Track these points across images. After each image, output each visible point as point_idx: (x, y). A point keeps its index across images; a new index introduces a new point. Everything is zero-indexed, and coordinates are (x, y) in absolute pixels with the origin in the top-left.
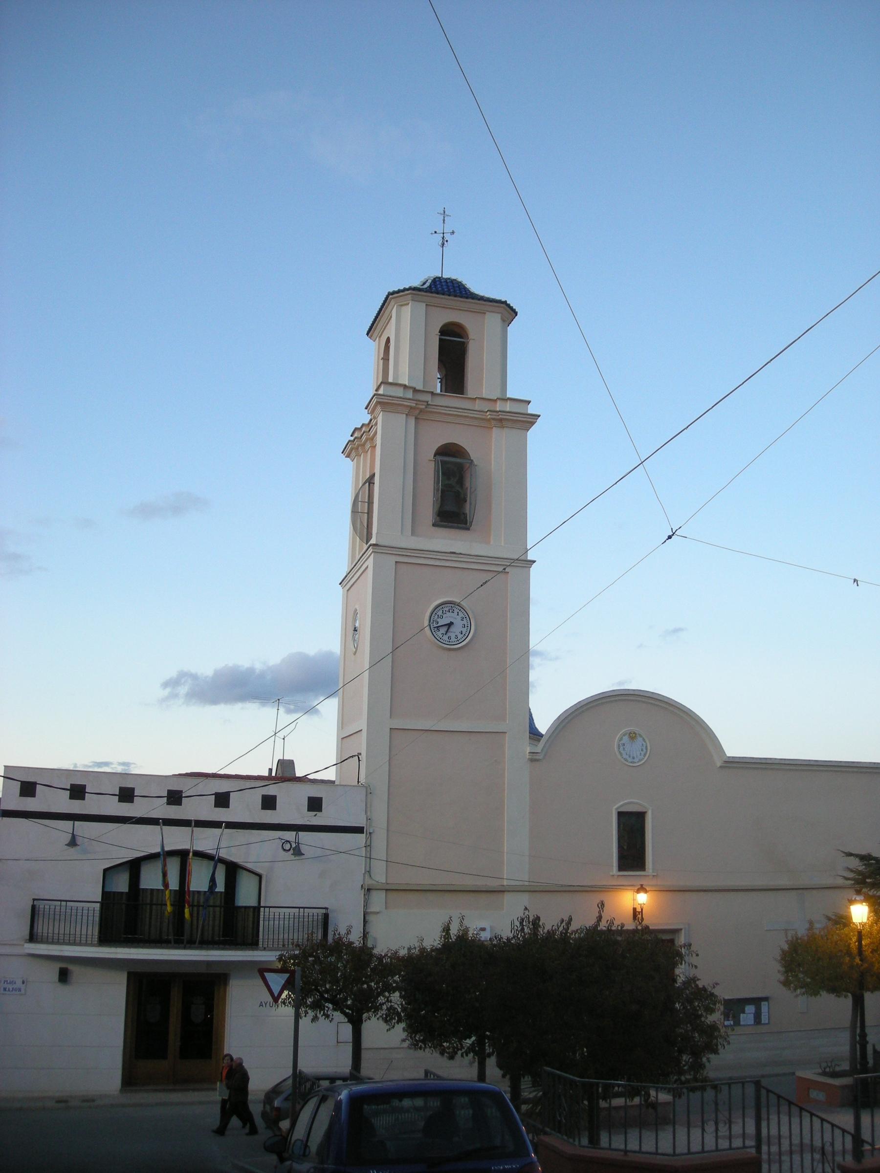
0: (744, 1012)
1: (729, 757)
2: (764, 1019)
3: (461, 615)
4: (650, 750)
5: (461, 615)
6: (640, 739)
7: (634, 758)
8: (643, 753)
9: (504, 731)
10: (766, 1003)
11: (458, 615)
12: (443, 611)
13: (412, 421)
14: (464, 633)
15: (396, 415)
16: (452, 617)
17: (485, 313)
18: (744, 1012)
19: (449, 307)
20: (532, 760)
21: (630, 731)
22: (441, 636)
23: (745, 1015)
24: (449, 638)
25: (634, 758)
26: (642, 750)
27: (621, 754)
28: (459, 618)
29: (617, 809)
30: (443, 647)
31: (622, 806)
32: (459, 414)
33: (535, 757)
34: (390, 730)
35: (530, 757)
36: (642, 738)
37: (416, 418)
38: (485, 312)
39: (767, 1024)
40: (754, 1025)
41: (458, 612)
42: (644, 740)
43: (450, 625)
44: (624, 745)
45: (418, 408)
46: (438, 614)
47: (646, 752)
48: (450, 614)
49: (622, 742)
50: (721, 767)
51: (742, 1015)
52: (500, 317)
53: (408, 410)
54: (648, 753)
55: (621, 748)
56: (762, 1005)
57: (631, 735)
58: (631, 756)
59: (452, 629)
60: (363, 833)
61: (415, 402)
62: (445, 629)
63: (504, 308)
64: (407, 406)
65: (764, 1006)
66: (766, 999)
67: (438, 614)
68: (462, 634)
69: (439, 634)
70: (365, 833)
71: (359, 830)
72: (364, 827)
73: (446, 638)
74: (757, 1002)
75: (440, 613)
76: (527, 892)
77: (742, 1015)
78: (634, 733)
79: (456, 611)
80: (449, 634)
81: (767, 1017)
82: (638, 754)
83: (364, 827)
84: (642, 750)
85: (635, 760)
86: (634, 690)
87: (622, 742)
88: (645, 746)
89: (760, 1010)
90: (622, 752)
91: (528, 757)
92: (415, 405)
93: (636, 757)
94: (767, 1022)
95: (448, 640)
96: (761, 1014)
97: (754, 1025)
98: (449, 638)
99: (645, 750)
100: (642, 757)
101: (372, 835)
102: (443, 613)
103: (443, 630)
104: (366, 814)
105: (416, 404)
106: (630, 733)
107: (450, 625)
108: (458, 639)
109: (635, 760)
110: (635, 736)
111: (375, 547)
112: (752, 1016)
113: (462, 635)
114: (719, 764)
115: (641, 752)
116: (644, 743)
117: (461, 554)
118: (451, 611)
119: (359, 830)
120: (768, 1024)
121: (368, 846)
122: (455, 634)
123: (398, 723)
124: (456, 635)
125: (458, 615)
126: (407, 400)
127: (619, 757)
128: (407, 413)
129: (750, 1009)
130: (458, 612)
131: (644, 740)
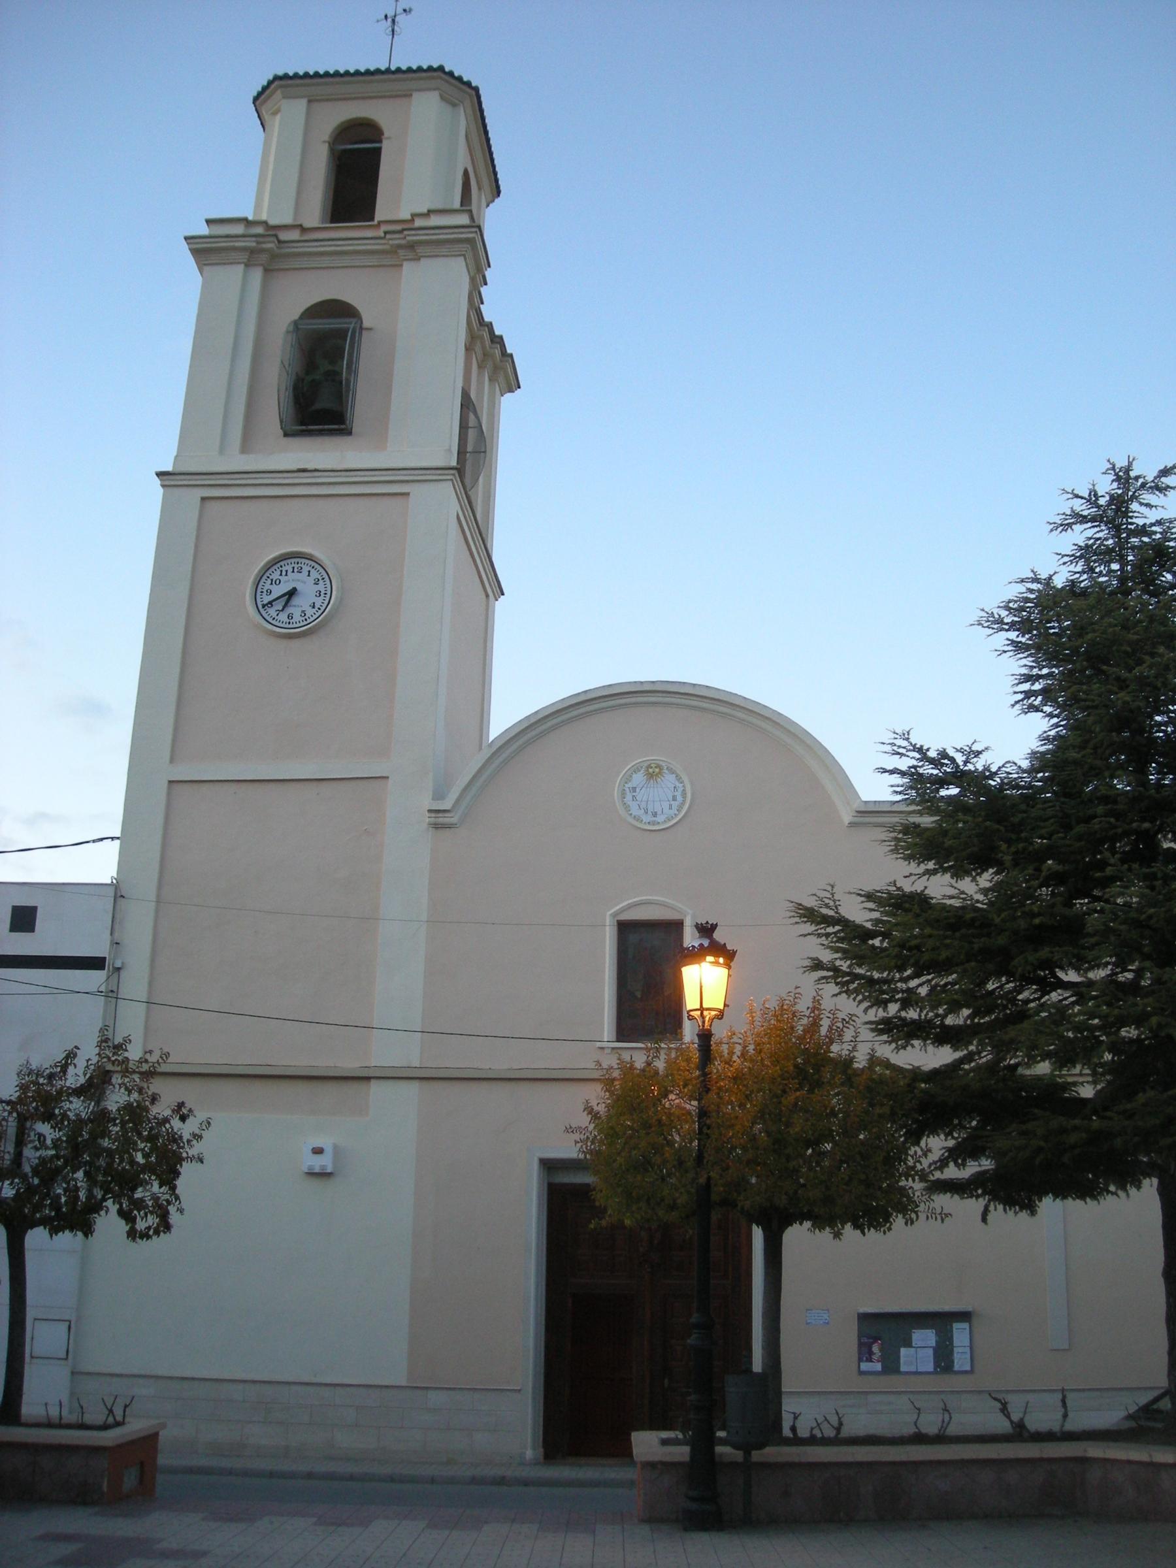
0: (908, 1344)
1: (866, 802)
2: (961, 1360)
3: (314, 574)
4: (693, 794)
5: (314, 574)
6: (672, 778)
7: (655, 814)
8: (675, 804)
9: (384, 775)
10: (966, 1325)
11: (309, 575)
12: (281, 571)
13: (257, 275)
14: (317, 606)
15: (228, 267)
16: (298, 580)
17: (411, 95)
18: (908, 1344)
19: (353, 96)
20: (437, 826)
21: (649, 763)
22: (274, 615)
23: (912, 1350)
24: (290, 616)
25: (655, 814)
26: (674, 798)
27: (627, 808)
28: (311, 580)
29: (614, 915)
30: (275, 632)
31: (630, 907)
32: (339, 249)
33: (441, 820)
34: (169, 788)
35: (432, 820)
36: (674, 775)
37: (267, 271)
38: (409, 93)
39: (966, 1372)
40: (935, 1372)
41: (309, 571)
42: (679, 778)
43: (292, 593)
44: (634, 789)
45: (262, 251)
46: (271, 577)
47: (683, 803)
48: (296, 575)
49: (630, 785)
50: (852, 825)
51: (903, 1351)
52: (438, 98)
53: (247, 257)
54: (687, 806)
55: (629, 796)
56: (954, 1329)
57: (651, 770)
58: (650, 809)
59: (296, 601)
60: (104, 969)
61: (254, 239)
62: (279, 605)
63: (441, 78)
64: (244, 249)
65: (960, 1334)
66: (964, 1316)
67: (271, 577)
68: (314, 607)
69: (272, 611)
70: (106, 968)
71: (95, 963)
72: (105, 958)
73: (283, 617)
74: (942, 1321)
75: (276, 576)
76: (418, 1080)
77: (903, 1351)
78: (658, 766)
79: (306, 569)
80: (289, 610)
81: (968, 1356)
82: (666, 805)
83: (105, 958)
84: (674, 798)
85: (660, 819)
86: (653, 682)
87: (630, 785)
88: (680, 790)
89: (951, 1339)
90: (630, 803)
91: (428, 820)
92: (254, 244)
93: (659, 813)
94: (968, 1368)
95: (288, 621)
96: (952, 1351)
97: (935, 1372)
98: (290, 616)
99: (679, 798)
100: (672, 812)
101: (123, 974)
102: (281, 575)
103: (279, 605)
104: (111, 934)
105: (258, 243)
106: (649, 767)
107: (292, 593)
108: (306, 617)
109: (660, 819)
110: (660, 773)
111: (165, 477)
112: (931, 1352)
113: (314, 610)
114: (847, 818)
115: (672, 802)
116: (678, 784)
117: (316, 470)
118: (296, 570)
119: (95, 963)
120: (972, 1372)
121: (112, 995)
122: (300, 609)
123: (183, 772)
124: (303, 611)
125: (309, 575)
126: (240, 239)
127: (622, 811)
128: (245, 260)
129: (924, 1338)
130: (309, 571)
131: (679, 778)
